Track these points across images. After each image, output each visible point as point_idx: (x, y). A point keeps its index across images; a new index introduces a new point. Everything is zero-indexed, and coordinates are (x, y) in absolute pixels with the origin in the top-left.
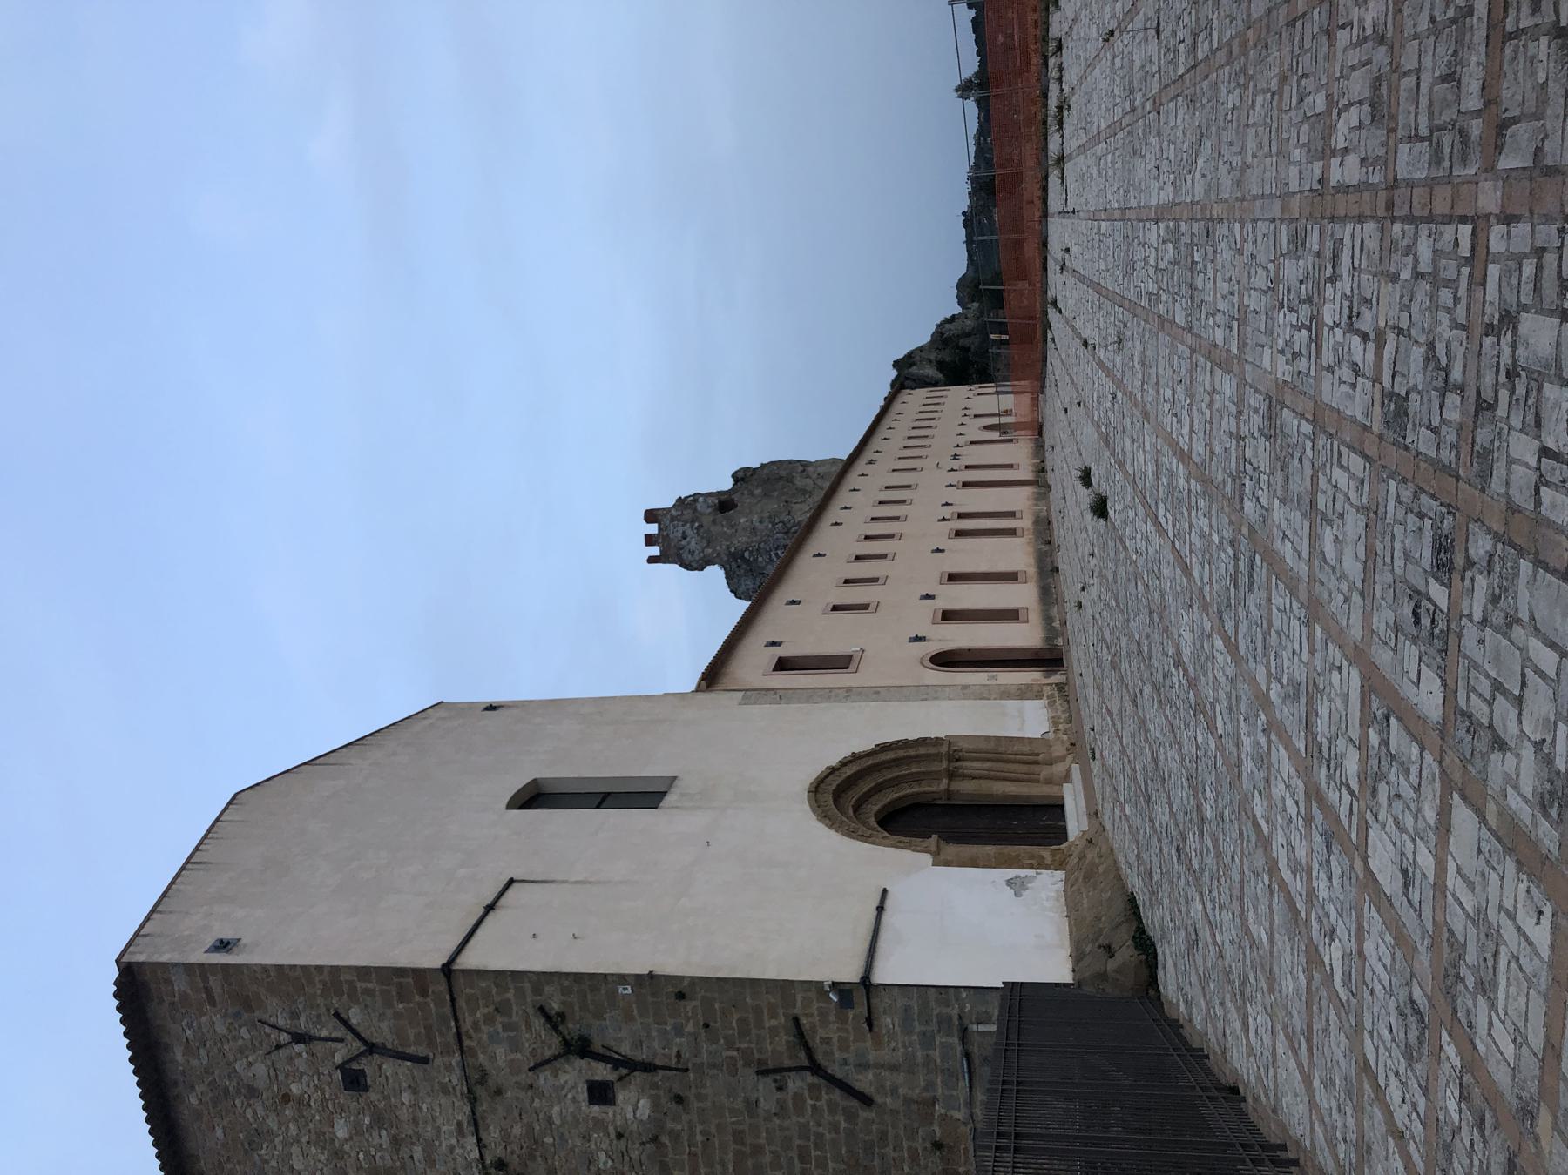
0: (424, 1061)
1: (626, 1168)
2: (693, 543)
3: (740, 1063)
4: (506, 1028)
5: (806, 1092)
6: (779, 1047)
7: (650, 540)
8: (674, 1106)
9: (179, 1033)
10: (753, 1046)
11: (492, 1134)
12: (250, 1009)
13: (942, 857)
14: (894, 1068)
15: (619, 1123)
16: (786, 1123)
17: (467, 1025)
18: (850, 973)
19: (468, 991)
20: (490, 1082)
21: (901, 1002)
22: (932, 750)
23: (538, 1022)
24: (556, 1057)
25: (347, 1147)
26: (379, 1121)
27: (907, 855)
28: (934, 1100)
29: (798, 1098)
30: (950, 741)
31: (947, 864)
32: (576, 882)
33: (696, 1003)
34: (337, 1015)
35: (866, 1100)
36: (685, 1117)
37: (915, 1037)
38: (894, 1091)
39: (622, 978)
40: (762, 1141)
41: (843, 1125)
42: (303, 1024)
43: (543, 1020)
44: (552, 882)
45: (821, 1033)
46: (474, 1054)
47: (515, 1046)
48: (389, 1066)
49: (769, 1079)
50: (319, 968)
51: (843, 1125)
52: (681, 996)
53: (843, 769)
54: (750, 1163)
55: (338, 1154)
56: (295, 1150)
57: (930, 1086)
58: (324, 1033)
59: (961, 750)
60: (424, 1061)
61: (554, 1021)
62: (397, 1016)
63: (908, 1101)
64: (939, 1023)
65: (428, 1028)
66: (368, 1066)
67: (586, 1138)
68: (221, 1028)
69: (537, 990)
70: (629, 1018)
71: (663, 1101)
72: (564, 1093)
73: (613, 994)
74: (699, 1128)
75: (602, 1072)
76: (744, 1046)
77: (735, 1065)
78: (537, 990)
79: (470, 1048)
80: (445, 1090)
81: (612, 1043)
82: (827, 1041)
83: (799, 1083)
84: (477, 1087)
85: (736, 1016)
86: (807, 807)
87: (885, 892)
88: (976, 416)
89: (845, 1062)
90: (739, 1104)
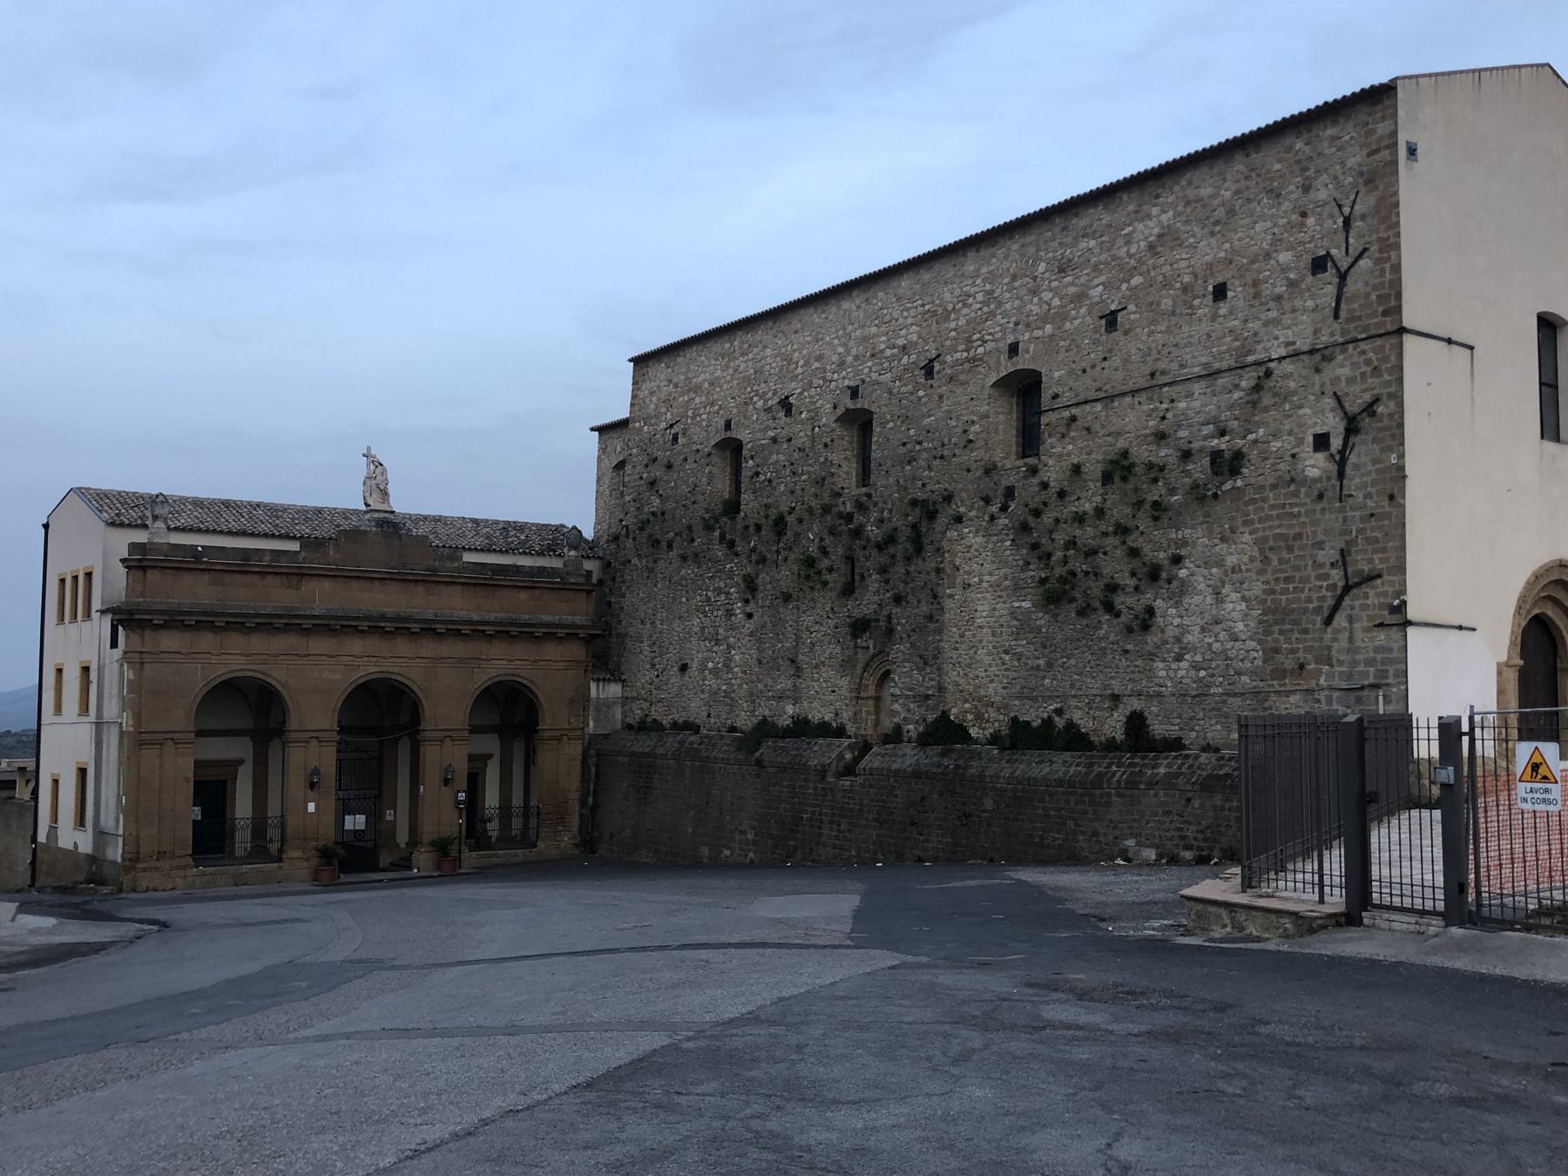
0: (1336, 316)
1: (1272, 461)
3: (1348, 538)
4: (1363, 374)
5: (1330, 582)
6: (1361, 562)
8: (1316, 493)
9: (1347, 131)
10: (1360, 547)
11: (1288, 366)
12: (1367, 183)
13: (1505, 669)
14: (1351, 640)
15: (1302, 455)
16: (1310, 568)
17: (1363, 346)
18: (1412, 613)
19: (1388, 346)
20: (1324, 364)
21: (1395, 646)
23: (1368, 397)
24: (1345, 413)
25: (1272, 262)
26: (1292, 284)
28: (1332, 666)
29: (1326, 577)
31: (1499, 673)
32: (1472, 397)
33: (1387, 509)
34: (1365, 250)
35: (1328, 621)
36: (1308, 500)
37: (1372, 654)
38: (1335, 640)
39: (1402, 456)
40: (1296, 553)
41: (1311, 606)
42: (1357, 224)
43: (1369, 401)
44: (1472, 378)
45: (1371, 593)
46: (1344, 351)
47: (1351, 381)
48: (1331, 290)
49: (1338, 557)
50: (1398, 235)
51: (1311, 606)
52: (1392, 497)
54: (1282, 544)
55: (1268, 255)
56: (1269, 224)
57: (1341, 663)
58: (1351, 240)
60: (1336, 316)
61: (1370, 409)
62: (1367, 295)
63: (1329, 648)
64: (1383, 671)
65: (1359, 318)
66: (1330, 275)
67: (1290, 433)
68: (1351, 162)
69: (1391, 396)
70: (1375, 461)
71: (1319, 485)
72: (1320, 416)
73: (1390, 449)
74: (1303, 510)
75: (1336, 443)
76: (1360, 541)
77: (1346, 534)
78: (1391, 396)
79: (1347, 350)
80: (1316, 332)
81: (1356, 450)
82: (1366, 596)
83: (1337, 577)
84: (1320, 355)
85: (1379, 535)
86: (1546, 561)
87: (1474, 630)
89: (1353, 608)
90: (1320, 537)
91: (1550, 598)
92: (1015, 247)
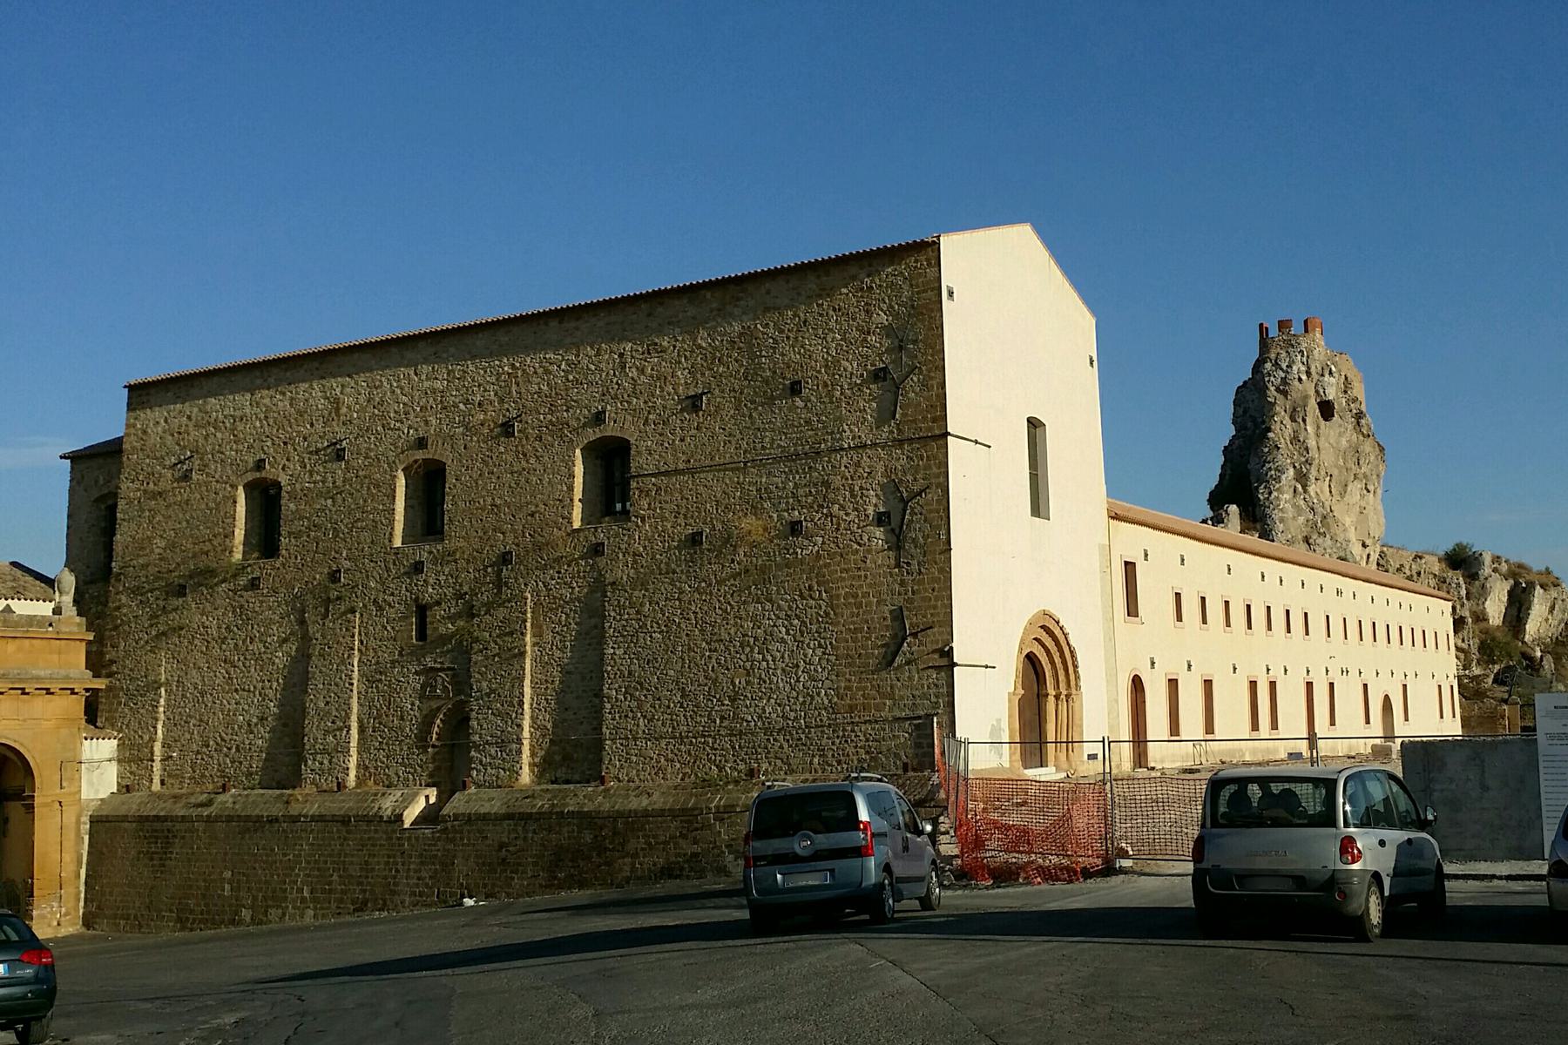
7: (1283, 325)
22: (1073, 683)
88: (1405, 686)
92: (600, 324)
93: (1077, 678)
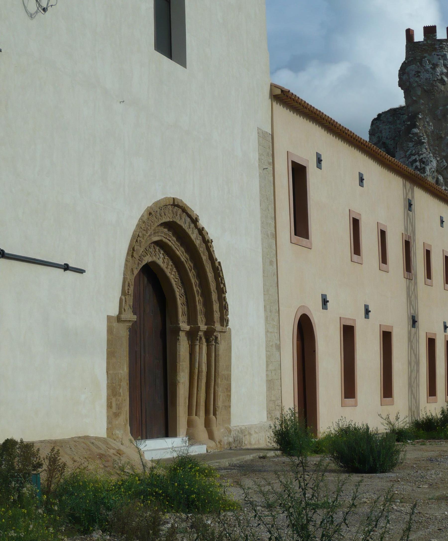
2: (427, 76)
22: (217, 316)
27: (117, 294)
30: (226, 333)
31: (110, 331)
53: (196, 231)
59: (216, 342)
91: (160, 244)
93: (224, 308)
